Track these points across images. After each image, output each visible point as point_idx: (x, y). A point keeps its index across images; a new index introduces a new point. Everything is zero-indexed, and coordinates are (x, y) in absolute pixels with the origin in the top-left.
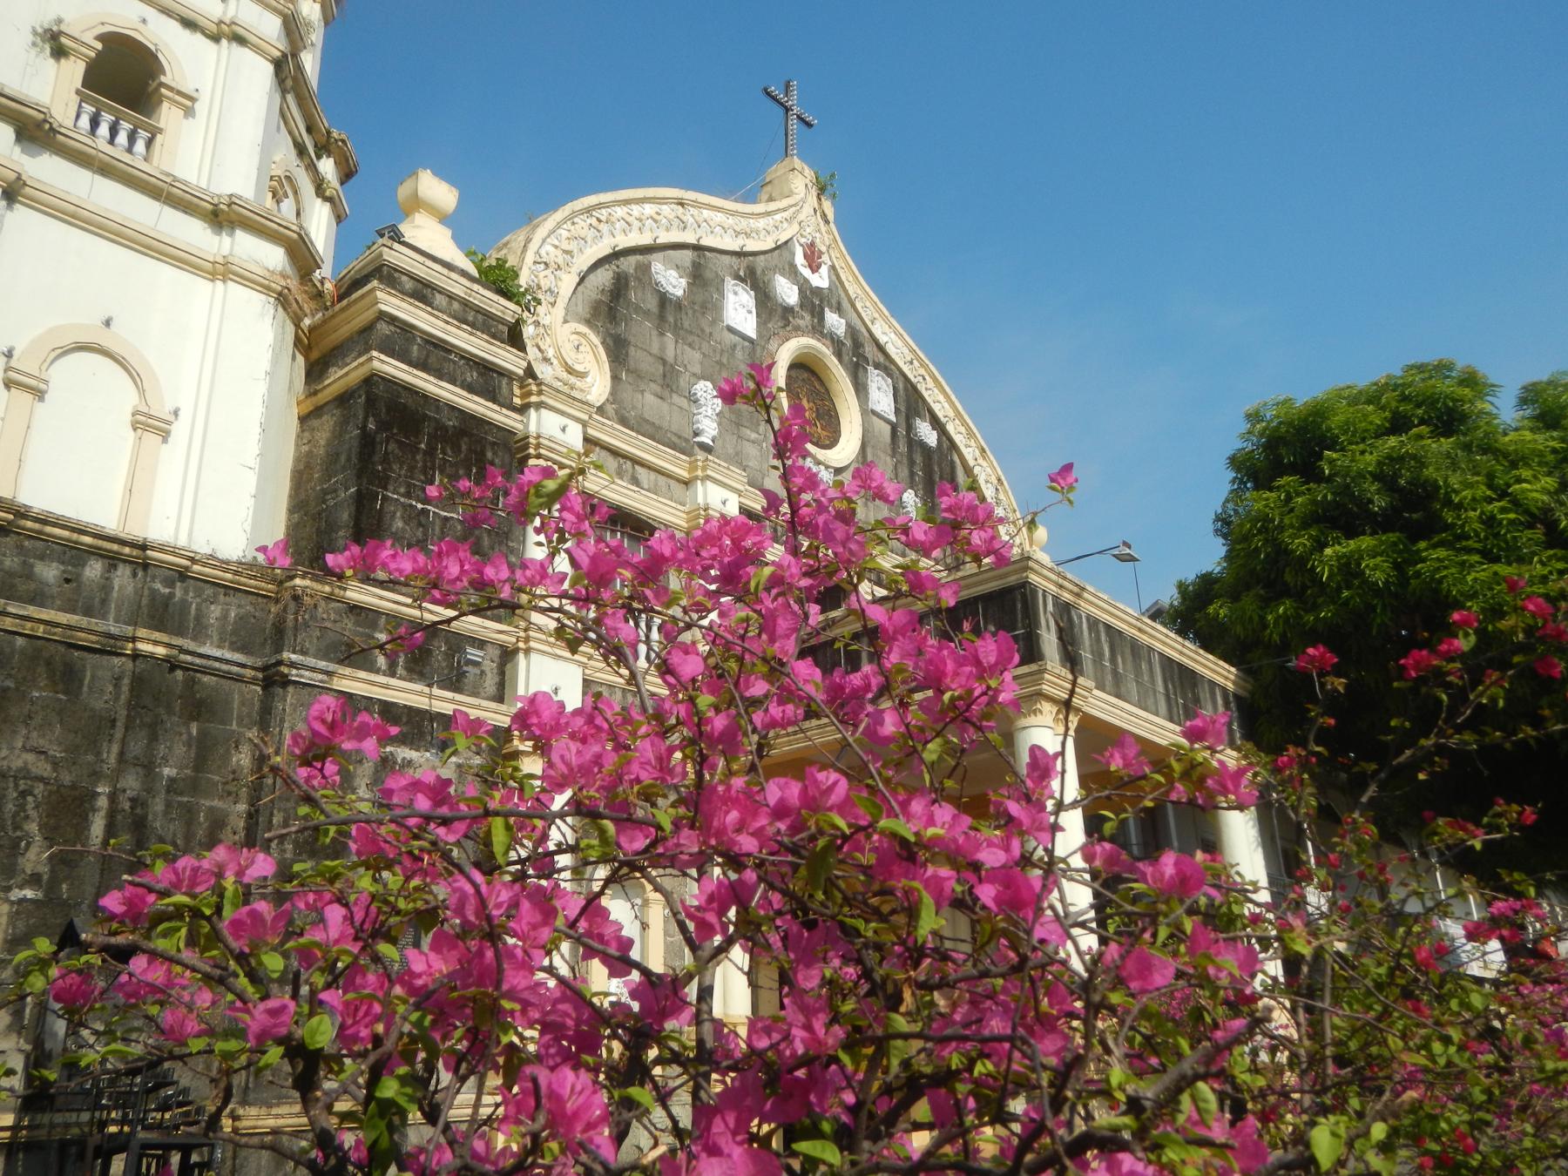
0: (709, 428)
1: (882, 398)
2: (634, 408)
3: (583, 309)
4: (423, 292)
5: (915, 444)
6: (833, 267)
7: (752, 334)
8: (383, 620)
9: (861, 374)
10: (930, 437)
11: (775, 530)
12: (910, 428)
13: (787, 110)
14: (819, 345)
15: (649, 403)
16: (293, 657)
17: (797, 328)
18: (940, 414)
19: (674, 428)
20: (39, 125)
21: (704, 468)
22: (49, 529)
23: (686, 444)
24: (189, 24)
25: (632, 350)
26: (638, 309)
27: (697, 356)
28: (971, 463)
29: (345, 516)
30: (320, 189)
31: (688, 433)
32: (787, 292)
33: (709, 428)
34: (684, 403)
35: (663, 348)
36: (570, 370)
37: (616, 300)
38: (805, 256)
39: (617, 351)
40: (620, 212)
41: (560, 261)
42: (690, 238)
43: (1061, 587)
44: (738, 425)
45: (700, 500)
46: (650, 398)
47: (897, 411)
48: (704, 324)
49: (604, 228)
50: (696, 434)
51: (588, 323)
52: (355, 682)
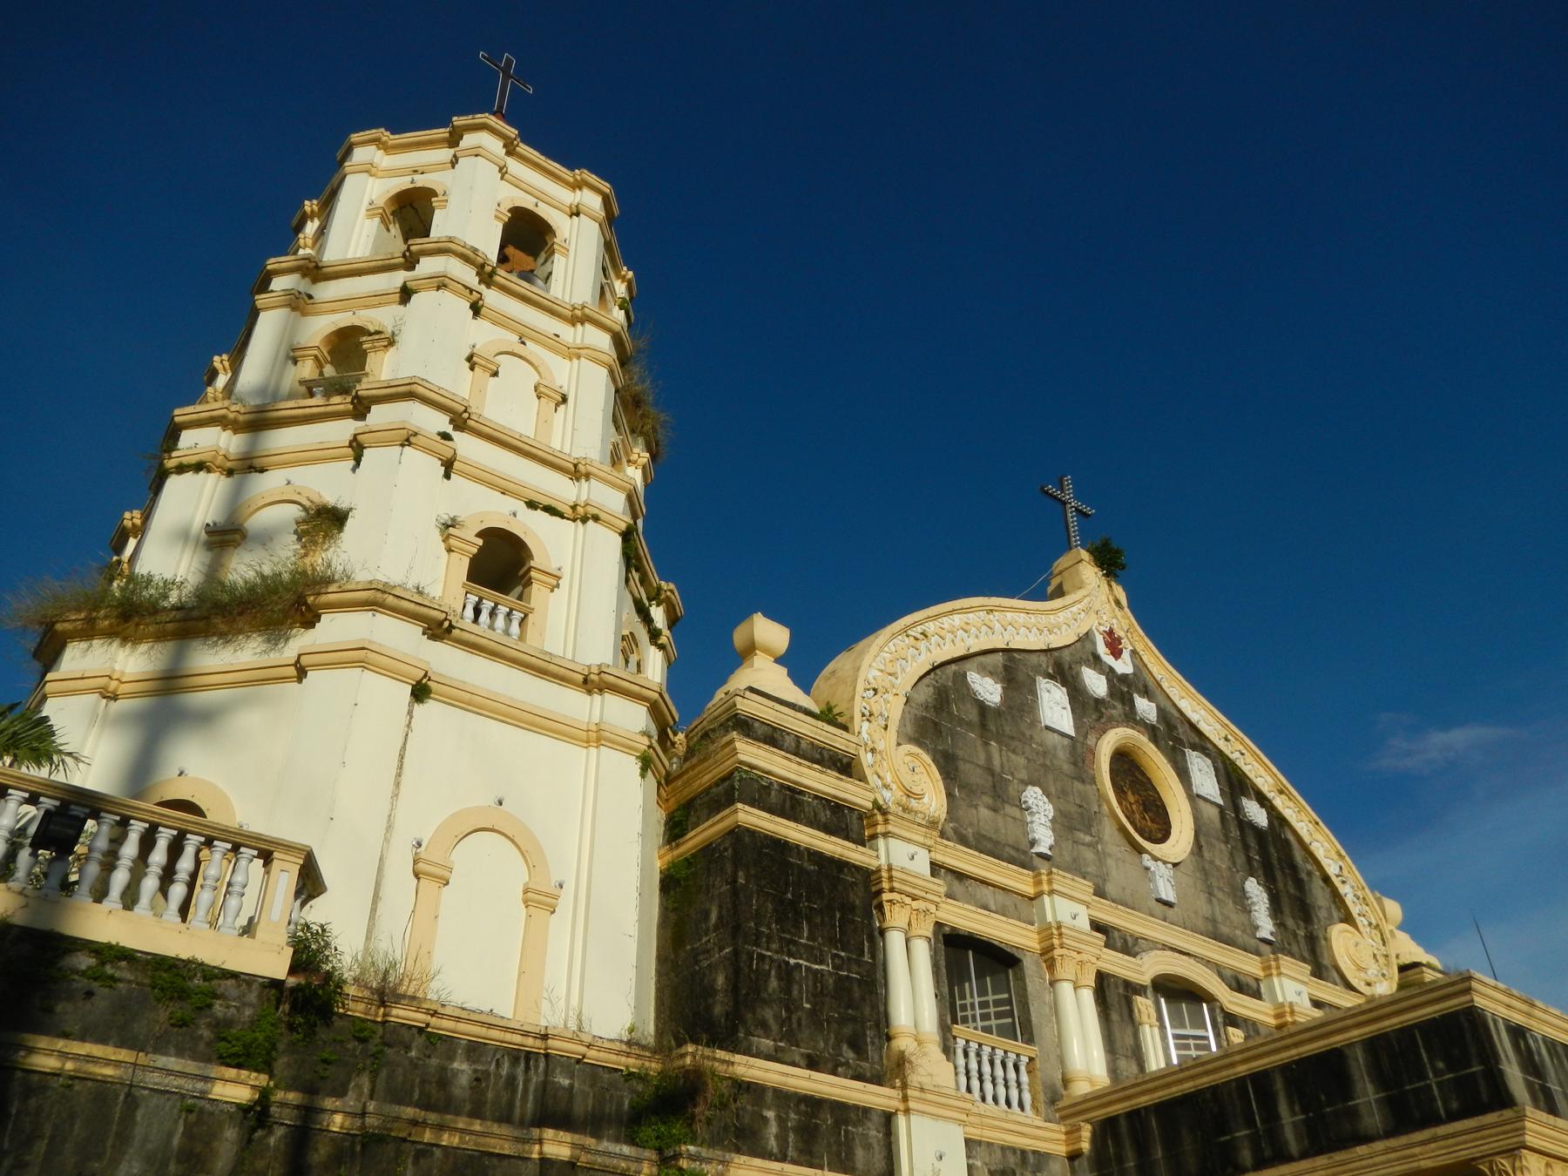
0: (1045, 838)
1: (1206, 782)
2: (971, 824)
4: (773, 737)
5: (1245, 825)
6: (1134, 653)
7: (1069, 729)
8: (770, 1094)
10: (1259, 816)
11: (1125, 941)
12: (1238, 809)
13: (1064, 503)
14: (1130, 731)
16: (691, 1148)
17: (1111, 719)
18: (1265, 789)
20: (441, 623)
21: (1050, 882)
22: (462, 1027)
23: (1021, 856)
24: (551, 510)
26: (961, 722)
27: (1021, 761)
28: (1307, 839)
29: (720, 980)
30: (654, 635)
31: (1024, 845)
32: (1097, 684)
33: (1045, 838)
34: (1015, 812)
35: (989, 758)
37: (941, 716)
38: (1107, 644)
39: (948, 766)
40: (931, 627)
41: (888, 685)
43: (1509, 1006)
44: (1071, 829)
45: (1050, 918)
46: (984, 812)
48: (1023, 727)
49: (922, 645)
50: (1033, 843)
51: (918, 742)
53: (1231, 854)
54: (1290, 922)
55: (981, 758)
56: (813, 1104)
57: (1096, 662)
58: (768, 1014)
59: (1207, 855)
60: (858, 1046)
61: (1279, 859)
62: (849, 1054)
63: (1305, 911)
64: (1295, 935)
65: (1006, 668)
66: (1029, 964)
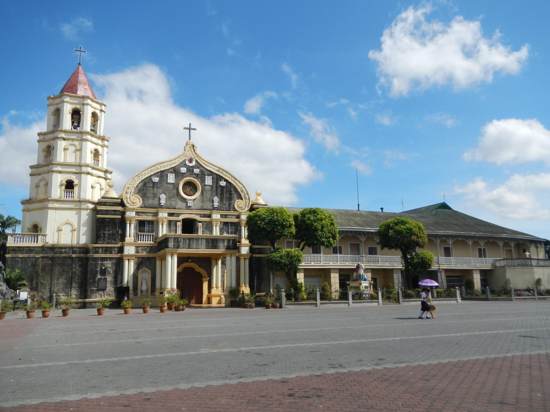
1: (209, 181)
9: (203, 179)
12: (217, 184)
15: (150, 202)
24: (76, 173)
26: (148, 187)
28: (236, 185)
32: (183, 170)
35: (154, 191)
42: (159, 170)
52: (96, 255)
54: (225, 202)
55: (152, 192)
56: (107, 248)
57: (186, 165)
59: (204, 194)
60: (115, 241)
62: (114, 241)
63: (230, 199)
66: (155, 222)
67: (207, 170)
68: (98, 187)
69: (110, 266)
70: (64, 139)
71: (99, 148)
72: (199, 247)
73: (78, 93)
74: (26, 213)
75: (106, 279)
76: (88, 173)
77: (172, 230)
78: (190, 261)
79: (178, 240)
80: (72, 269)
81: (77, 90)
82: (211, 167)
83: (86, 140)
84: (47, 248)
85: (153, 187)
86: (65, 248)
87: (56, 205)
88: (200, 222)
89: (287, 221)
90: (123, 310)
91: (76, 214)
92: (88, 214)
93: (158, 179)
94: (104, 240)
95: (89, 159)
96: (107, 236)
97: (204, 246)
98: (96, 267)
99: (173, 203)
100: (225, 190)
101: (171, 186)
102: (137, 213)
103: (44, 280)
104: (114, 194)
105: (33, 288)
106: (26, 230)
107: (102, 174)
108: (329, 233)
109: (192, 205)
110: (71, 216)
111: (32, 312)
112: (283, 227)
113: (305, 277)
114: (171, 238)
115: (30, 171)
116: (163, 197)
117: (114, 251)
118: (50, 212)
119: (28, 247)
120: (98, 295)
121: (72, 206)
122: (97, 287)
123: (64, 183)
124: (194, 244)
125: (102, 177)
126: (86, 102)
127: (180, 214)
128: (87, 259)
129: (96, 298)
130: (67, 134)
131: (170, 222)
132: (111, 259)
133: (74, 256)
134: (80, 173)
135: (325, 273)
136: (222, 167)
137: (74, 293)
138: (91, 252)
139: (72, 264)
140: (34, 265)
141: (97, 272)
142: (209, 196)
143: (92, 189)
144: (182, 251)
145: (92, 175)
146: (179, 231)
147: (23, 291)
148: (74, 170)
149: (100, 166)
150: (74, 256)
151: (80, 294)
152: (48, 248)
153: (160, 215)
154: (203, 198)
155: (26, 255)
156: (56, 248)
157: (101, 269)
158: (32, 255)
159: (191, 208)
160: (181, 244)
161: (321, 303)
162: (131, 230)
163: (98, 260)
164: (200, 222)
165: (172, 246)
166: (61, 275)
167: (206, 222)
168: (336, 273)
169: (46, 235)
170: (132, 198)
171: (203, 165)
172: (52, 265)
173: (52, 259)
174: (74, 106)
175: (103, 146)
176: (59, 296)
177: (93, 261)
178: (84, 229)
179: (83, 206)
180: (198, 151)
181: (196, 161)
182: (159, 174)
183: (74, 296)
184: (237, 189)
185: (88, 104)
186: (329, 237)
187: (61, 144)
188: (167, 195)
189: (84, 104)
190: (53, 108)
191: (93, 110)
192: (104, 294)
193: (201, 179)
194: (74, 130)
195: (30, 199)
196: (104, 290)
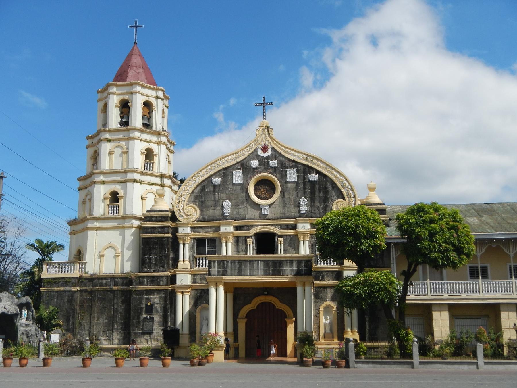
1: (292, 175)
3: (193, 200)
9: (284, 173)
12: (304, 178)
15: (211, 212)
19: (218, 214)
24: (121, 182)
25: (206, 202)
26: (207, 192)
32: (255, 163)
35: (215, 198)
36: (188, 215)
40: (201, 173)
42: (221, 168)
47: (298, 176)
51: (194, 202)
52: (140, 288)
53: (297, 194)
54: (317, 204)
55: (213, 199)
57: (257, 157)
58: (147, 266)
59: (286, 196)
60: (163, 267)
61: (319, 189)
62: (162, 268)
63: (326, 199)
64: (318, 208)
65: (224, 173)
66: (217, 240)
67: (289, 160)
68: (151, 198)
69: (158, 302)
70: (109, 141)
71: (154, 147)
72: (255, 273)
73: (128, 80)
74: (73, 235)
75: (153, 318)
76: (135, 181)
77: (240, 250)
78: (266, 293)
79: (224, 264)
80: (114, 306)
81: (126, 77)
82: (294, 156)
83: (133, 138)
84: (85, 278)
85: (214, 191)
86: (106, 278)
87: (97, 224)
88: (281, 236)
89: (363, 227)
90: (160, 362)
91: (120, 234)
92: (133, 234)
93: (220, 179)
94: (150, 267)
95: (138, 162)
96: (153, 261)
97: (261, 272)
98: (141, 303)
99: (242, 212)
100: (317, 186)
101: (238, 188)
102: (193, 229)
103: (82, 319)
104: (165, 205)
105: (70, 329)
106: (72, 256)
107: (157, 180)
108: (446, 242)
109: (268, 213)
110: (113, 237)
111: (8, 359)
112: (357, 237)
113: (453, 317)
114: (214, 261)
115: (78, 184)
116: (227, 204)
117: (163, 281)
118: (90, 233)
119: (64, 278)
120: (143, 340)
121: (114, 224)
122: (142, 329)
123: (108, 195)
124: (247, 269)
125: (157, 185)
126: (134, 90)
127: (252, 226)
128: (130, 291)
129: (143, 344)
130: (113, 133)
131: (237, 239)
132: (159, 291)
133: (115, 288)
134: (125, 181)
135: (491, 312)
136: (311, 154)
137: (117, 336)
138: (134, 283)
139: (114, 299)
140: (71, 301)
141: (141, 309)
142: (292, 197)
143: (140, 200)
144: (228, 279)
145: (141, 183)
146: (251, 252)
147: (55, 333)
148: (118, 178)
149: (156, 169)
150: (115, 288)
151: (124, 339)
152: (86, 279)
153: (223, 229)
154: (284, 201)
155: (62, 289)
156: (95, 279)
157: (147, 305)
158: (68, 288)
159: (268, 217)
160: (228, 270)
161: (421, 363)
162: (185, 252)
163: (143, 293)
164: (281, 236)
165: (216, 273)
166: (101, 313)
167: (289, 235)
168: (511, 311)
169: (85, 263)
170: (186, 208)
171: (283, 153)
172: (91, 300)
173: (91, 292)
174: (121, 97)
175: (159, 144)
176: (99, 340)
177: (137, 295)
178: (128, 254)
179: (127, 224)
180: (274, 134)
181: (273, 149)
182: (222, 172)
183: (116, 341)
184: (336, 184)
185: (136, 92)
186: (447, 250)
187: (106, 147)
188: (233, 201)
189: (132, 93)
190: (101, 104)
191: (145, 99)
192: (151, 339)
193: (281, 174)
194: (122, 128)
195: (75, 219)
196: (150, 333)
